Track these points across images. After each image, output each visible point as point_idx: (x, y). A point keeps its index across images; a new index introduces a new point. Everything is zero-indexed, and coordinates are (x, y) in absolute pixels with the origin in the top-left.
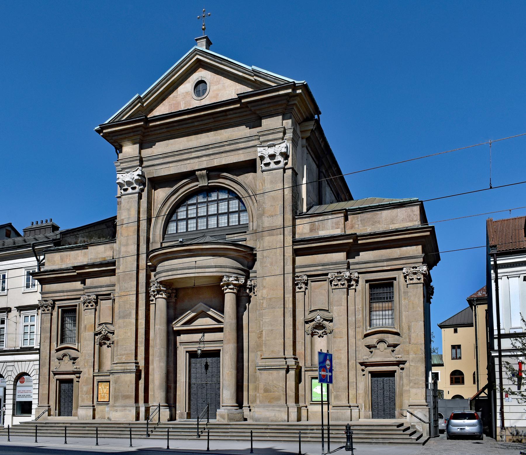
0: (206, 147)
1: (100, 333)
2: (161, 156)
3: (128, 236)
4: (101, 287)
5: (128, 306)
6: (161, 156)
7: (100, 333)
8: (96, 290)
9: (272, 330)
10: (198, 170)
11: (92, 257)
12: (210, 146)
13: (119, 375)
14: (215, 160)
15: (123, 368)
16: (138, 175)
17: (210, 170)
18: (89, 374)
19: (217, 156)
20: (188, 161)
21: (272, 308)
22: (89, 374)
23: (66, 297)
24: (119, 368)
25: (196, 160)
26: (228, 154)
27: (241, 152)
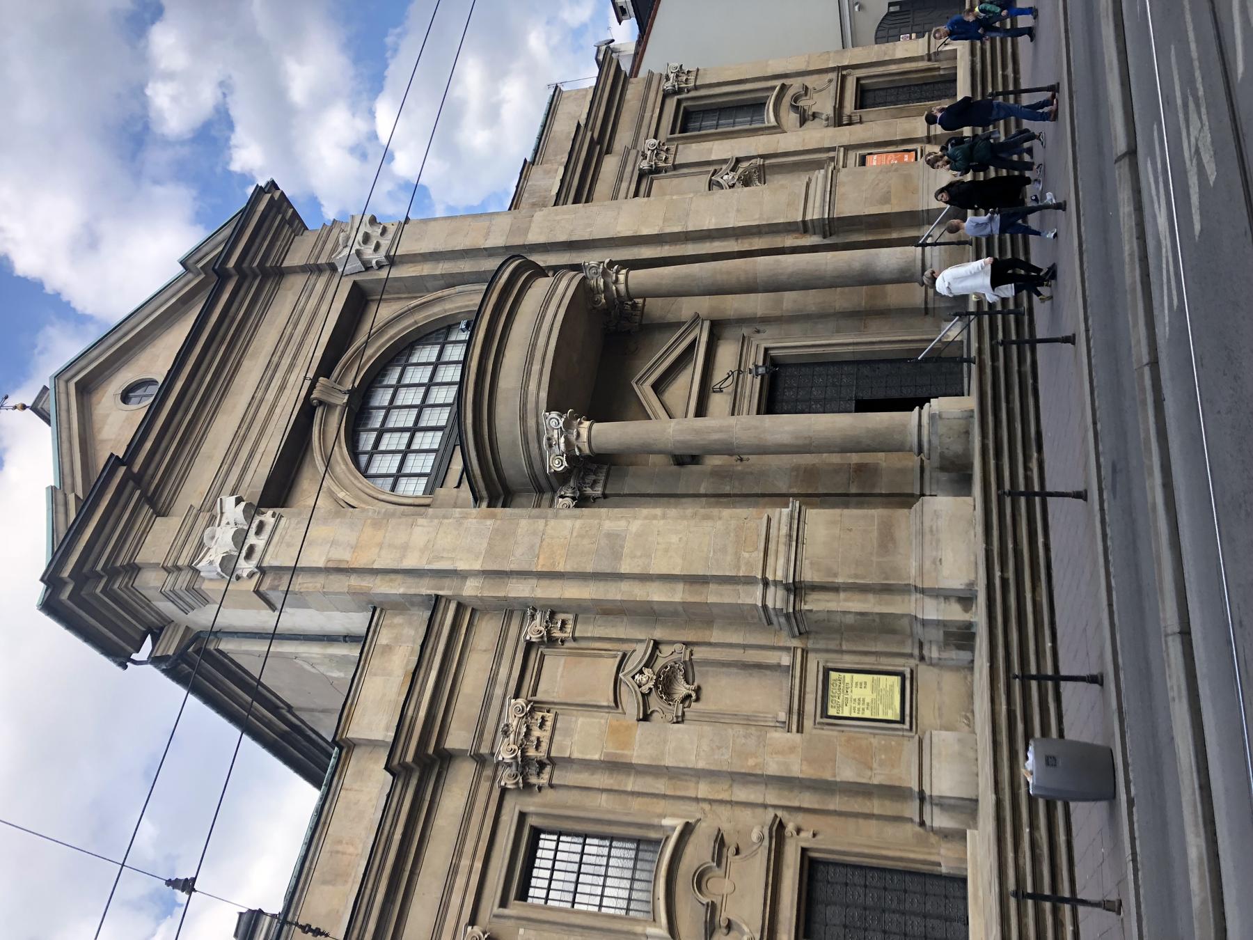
0: (271, 368)
2: (225, 467)
3: (381, 546)
4: (492, 681)
5: (586, 542)
6: (225, 467)
8: (499, 691)
9: (738, 211)
12: (275, 359)
13: (806, 563)
15: (782, 548)
16: (238, 501)
17: (326, 367)
18: (792, 749)
21: (688, 215)
22: (792, 749)
23: (478, 865)
24: (781, 561)
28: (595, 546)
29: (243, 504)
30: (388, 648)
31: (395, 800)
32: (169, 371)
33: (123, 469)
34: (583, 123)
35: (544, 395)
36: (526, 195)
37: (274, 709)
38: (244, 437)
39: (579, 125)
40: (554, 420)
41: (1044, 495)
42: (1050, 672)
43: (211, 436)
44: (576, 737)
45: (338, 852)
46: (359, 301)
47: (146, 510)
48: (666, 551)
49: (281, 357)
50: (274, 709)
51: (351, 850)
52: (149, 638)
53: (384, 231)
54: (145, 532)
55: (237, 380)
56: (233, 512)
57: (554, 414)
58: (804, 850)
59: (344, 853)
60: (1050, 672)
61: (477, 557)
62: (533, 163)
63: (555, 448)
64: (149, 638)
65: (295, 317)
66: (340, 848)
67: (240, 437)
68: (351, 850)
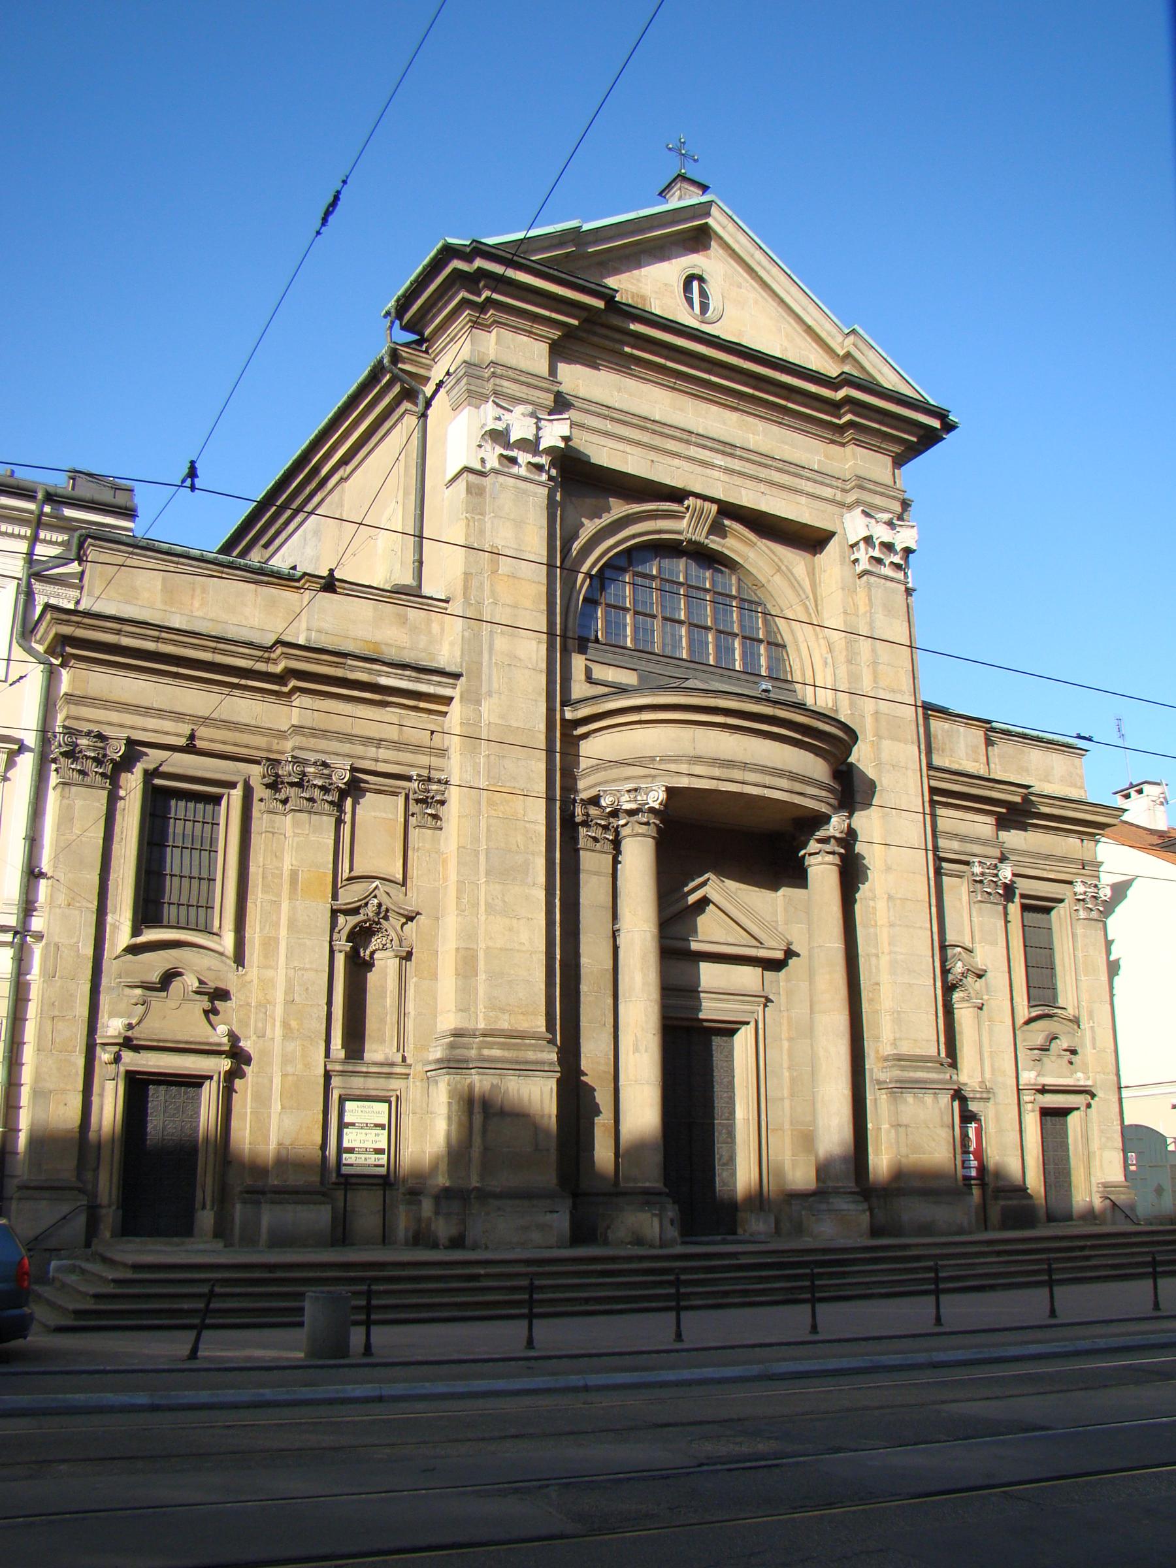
0: (727, 448)
1: (355, 911)
3: (515, 607)
7: (355, 911)
8: (359, 750)
10: (697, 496)
11: (325, 626)
14: (744, 492)
16: (566, 439)
17: (728, 510)
18: (307, 1066)
19: (749, 483)
20: (676, 462)
22: (307, 1066)
25: (699, 469)
26: (775, 491)
27: (803, 500)
28: (514, 848)
29: (562, 445)
30: (404, 620)
31: (247, 651)
32: (718, 337)
33: (601, 304)
34: (1031, 790)
35: (684, 782)
36: (946, 726)
37: (344, 461)
38: (645, 429)
39: (1030, 787)
40: (656, 797)
41: (531, 1317)
42: (374, 1317)
43: (648, 388)
44: (313, 838)
45: (194, 590)
46: (812, 540)
47: (555, 334)
48: (511, 930)
49: (741, 458)
50: (344, 461)
51: (197, 604)
52: (417, 337)
53: (898, 567)
54: (530, 333)
55: (714, 409)
56: (554, 434)
57: (662, 796)
58: (211, 1078)
59: (193, 597)
60: (374, 1317)
61: (502, 717)
62: (993, 730)
63: (626, 797)
64: (417, 337)
65: (792, 469)
66: (198, 591)
67: (645, 423)
68: (197, 604)
